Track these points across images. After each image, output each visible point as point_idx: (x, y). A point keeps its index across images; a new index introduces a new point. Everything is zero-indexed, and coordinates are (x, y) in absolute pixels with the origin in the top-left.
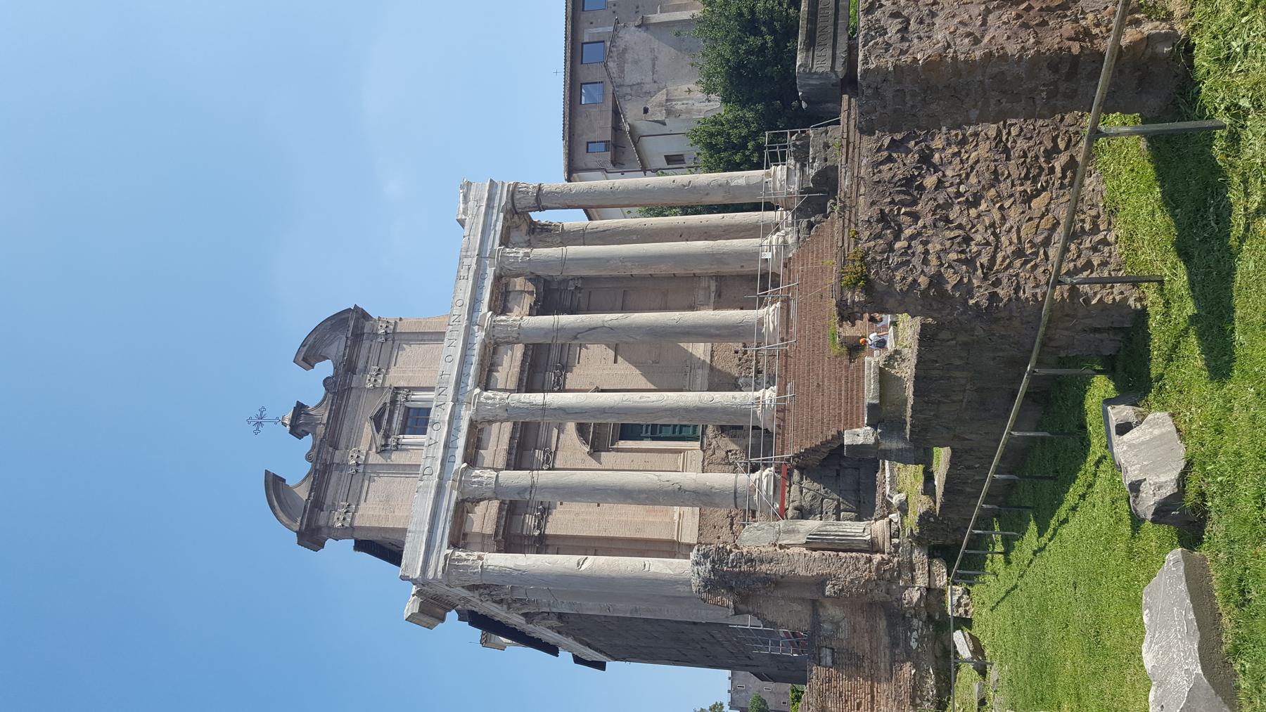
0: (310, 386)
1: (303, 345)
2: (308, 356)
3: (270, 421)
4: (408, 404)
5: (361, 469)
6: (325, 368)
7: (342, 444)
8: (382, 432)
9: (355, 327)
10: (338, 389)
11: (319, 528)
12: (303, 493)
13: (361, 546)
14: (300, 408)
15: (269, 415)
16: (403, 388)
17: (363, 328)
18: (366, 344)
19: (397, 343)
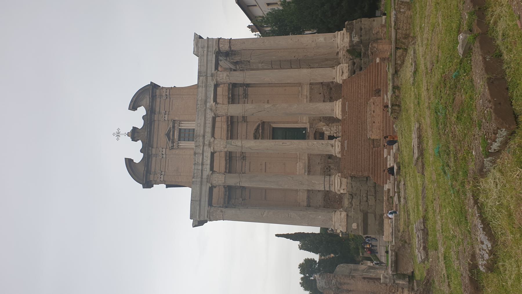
0: (137, 118)
1: (131, 102)
2: (133, 106)
3: (122, 134)
4: (180, 127)
5: (164, 156)
6: (142, 111)
7: (155, 146)
9: (152, 93)
10: (148, 119)
12: (142, 169)
13: (167, 186)
14: (135, 129)
15: (122, 131)
17: (156, 93)
18: (158, 100)
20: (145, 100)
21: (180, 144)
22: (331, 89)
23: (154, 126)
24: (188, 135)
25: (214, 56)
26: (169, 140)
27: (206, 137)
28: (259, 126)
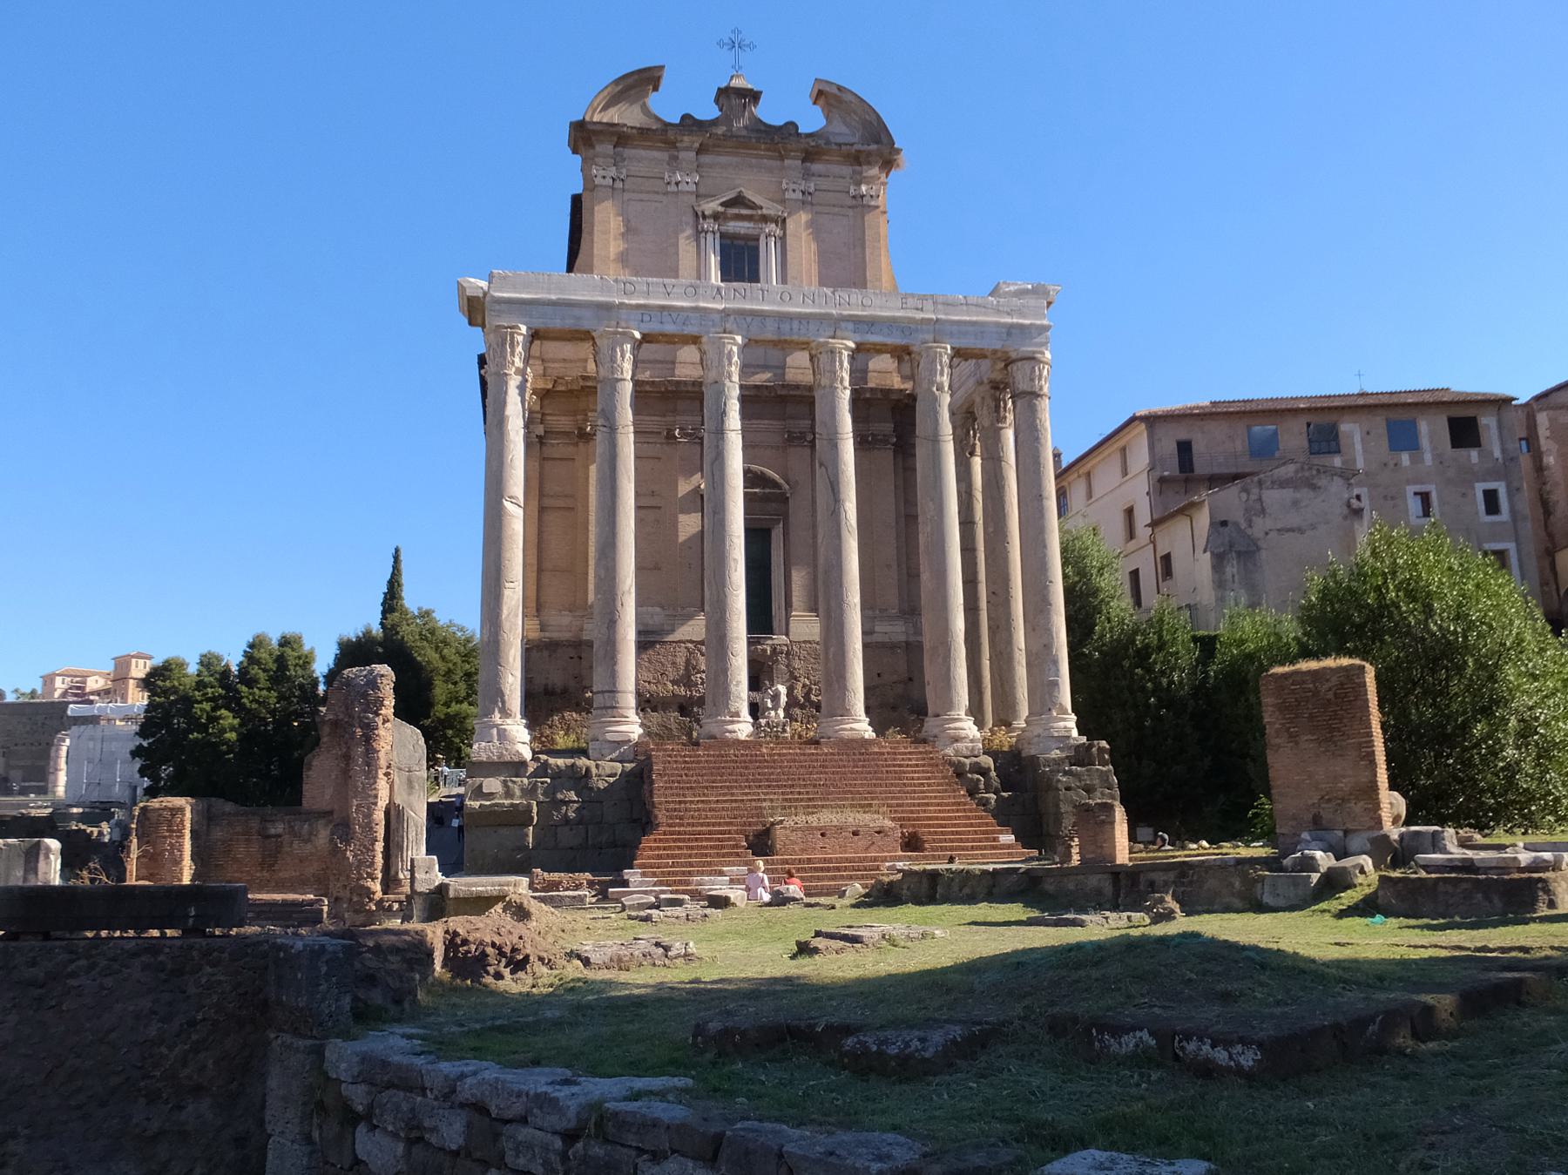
0: (788, 104)
1: (840, 88)
2: (825, 95)
4: (762, 238)
5: (673, 188)
6: (811, 120)
7: (706, 159)
8: (721, 209)
9: (869, 154)
11: (592, 146)
13: (577, 201)
14: (755, 96)
16: (784, 229)
17: (869, 163)
18: (846, 170)
19: (851, 213)
20: (844, 129)
21: (710, 237)
22: (894, 708)
23: (762, 157)
24: (740, 262)
25: (998, 345)
26: (722, 204)
27: (749, 319)
28: (775, 485)
